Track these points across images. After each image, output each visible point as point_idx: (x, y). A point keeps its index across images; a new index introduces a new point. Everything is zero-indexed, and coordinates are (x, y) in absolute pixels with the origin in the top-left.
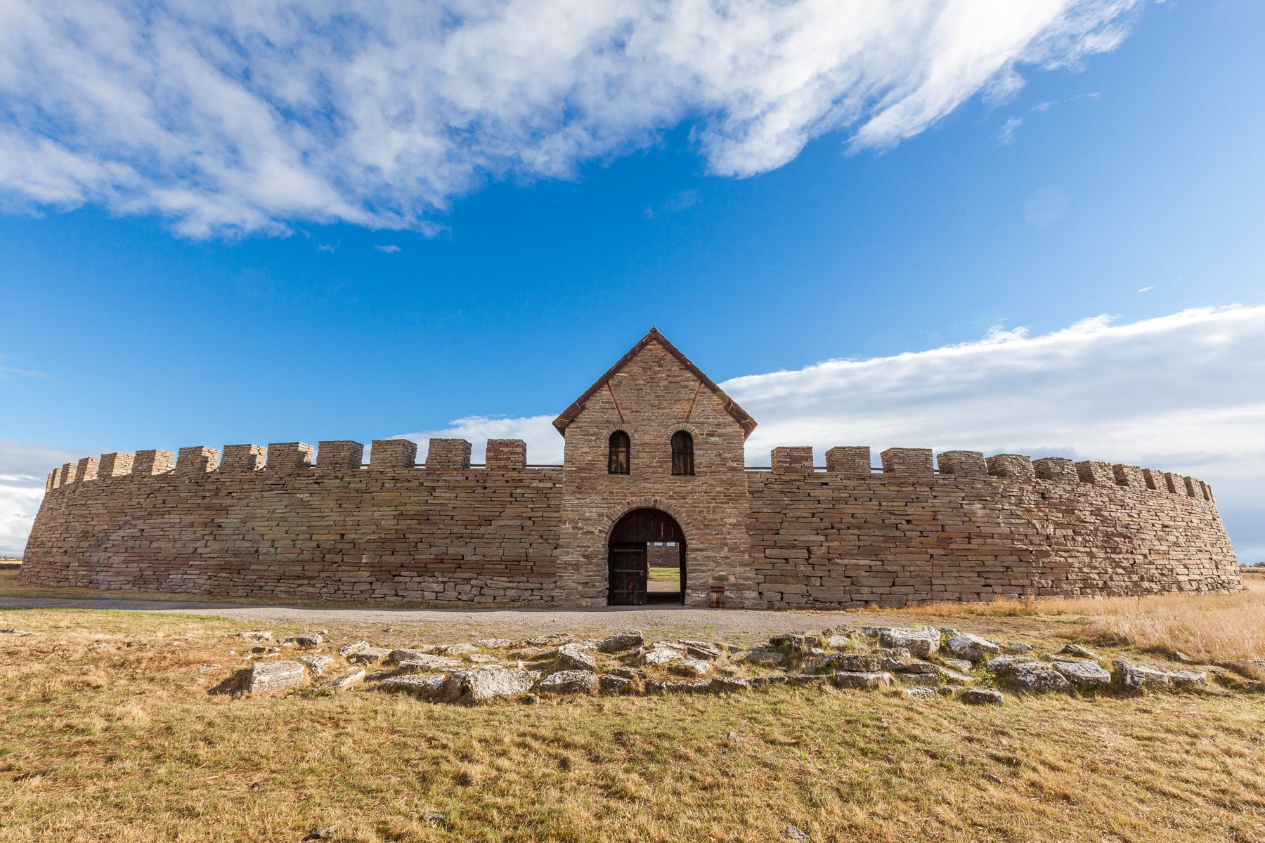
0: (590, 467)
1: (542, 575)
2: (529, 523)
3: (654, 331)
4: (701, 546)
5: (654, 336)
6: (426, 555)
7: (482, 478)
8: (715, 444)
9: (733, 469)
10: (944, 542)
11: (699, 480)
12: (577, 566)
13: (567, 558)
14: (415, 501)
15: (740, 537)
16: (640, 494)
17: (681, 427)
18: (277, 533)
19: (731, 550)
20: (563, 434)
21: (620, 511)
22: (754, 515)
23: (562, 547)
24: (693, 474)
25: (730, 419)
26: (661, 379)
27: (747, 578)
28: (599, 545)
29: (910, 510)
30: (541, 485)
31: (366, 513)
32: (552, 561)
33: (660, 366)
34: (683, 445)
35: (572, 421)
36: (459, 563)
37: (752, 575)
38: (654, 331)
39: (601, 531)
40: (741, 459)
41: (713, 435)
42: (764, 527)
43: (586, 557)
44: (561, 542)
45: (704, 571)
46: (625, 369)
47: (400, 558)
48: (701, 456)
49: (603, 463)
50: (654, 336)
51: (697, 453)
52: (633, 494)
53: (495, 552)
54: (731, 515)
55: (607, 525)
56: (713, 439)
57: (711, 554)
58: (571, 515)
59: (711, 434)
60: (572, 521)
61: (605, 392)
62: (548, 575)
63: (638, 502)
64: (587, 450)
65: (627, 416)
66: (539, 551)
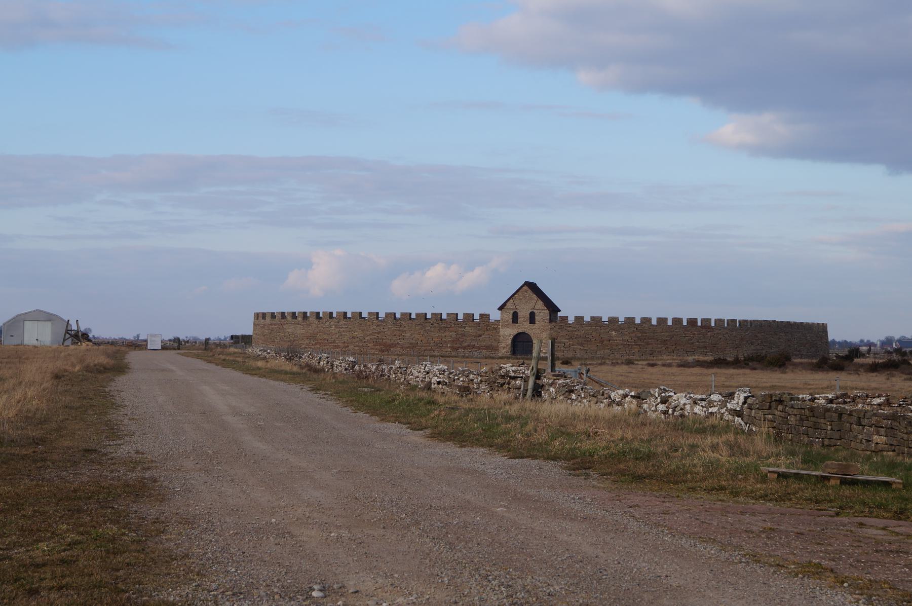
6: (466, 344)
7: (478, 324)
10: (602, 342)
14: (460, 330)
18: (422, 338)
21: (515, 333)
22: (551, 334)
28: (509, 342)
29: (594, 334)
31: (447, 333)
36: (474, 347)
47: (458, 345)
48: (537, 319)
53: (483, 344)
54: (545, 335)
63: (520, 331)
66: (495, 344)
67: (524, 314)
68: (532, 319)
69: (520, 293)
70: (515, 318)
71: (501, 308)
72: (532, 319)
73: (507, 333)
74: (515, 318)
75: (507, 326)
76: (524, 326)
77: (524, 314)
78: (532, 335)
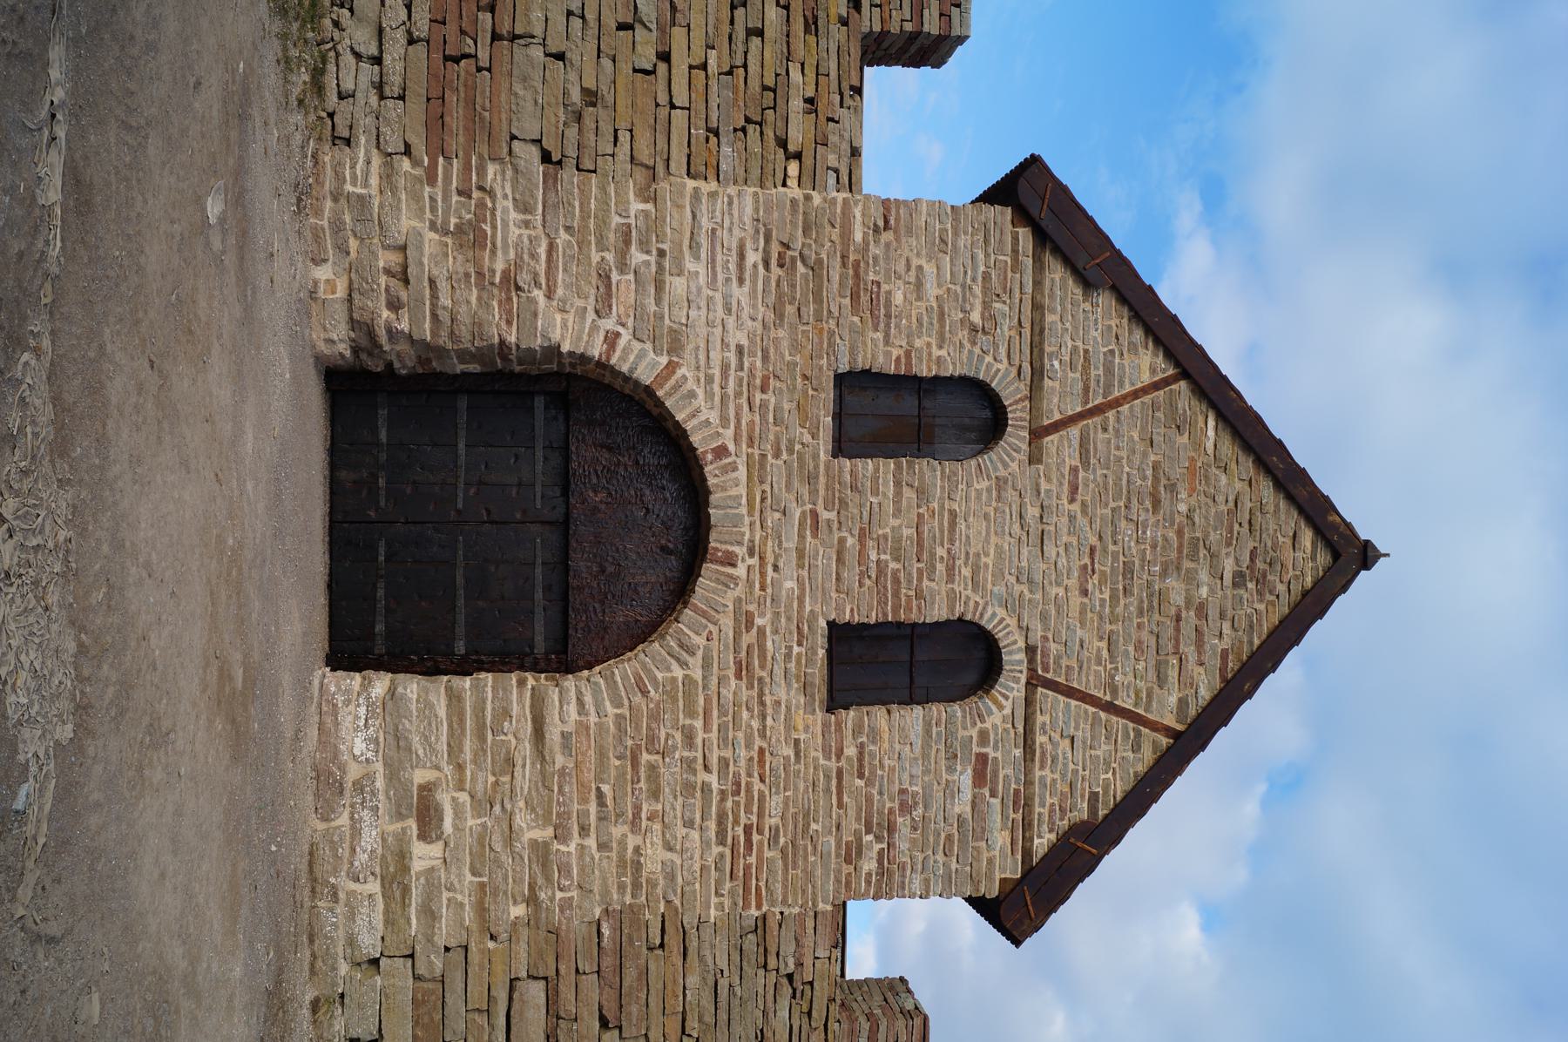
0: (866, 298)
1: (437, 100)
2: (647, 57)
3: (1366, 556)
4: (553, 734)
5: (1349, 555)
8: (950, 791)
9: (852, 853)
11: (811, 722)
12: (472, 237)
13: (505, 207)
15: (584, 894)
16: (762, 504)
17: (1014, 657)
19: (541, 852)
20: (991, 196)
21: (701, 416)
22: (675, 936)
23: (550, 181)
24: (834, 704)
25: (1042, 842)
26: (1190, 579)
27: (429, 914)
28: (566, 326)
30: (797, 104)
32: (489, 137)
33: (1239, 580)
34: (955, 659)
35: (1042, 238)
37: (445, 933)
38: (1366, 556)
39: (612, 339)
40: (886, 885)
41: (979, 778)
42: (630, 974)
43: (510, 283)
44: (568, 175)
45: (454, 750)
46: (1228, 448)
48: (901, 732)
49: (881, 354)
50: (1349, 555)
51: (914, 716)
52: (758, 469)
54: (675, 854)
55: (640, 362)
56: (966, 779)
57: (525, 776)
58: (677, 220)
59: (982, 771)
60: (654, 225)
61: (1146, 364)
62: (436, 123)
63: (728, 488)
64: (932, 290)
65: (1062, 449)
66: (530, 98)
67: (964, 535)
68: (901, 660)
69: (1235, 477)
70: (906, 415)
71: (1029, 197)
72: (901, 660)
73: (688, 304)
74: (906, 415)
75: (793, 266)
76: (795, 535)
77: (964, 535)
78: (655, 663)
